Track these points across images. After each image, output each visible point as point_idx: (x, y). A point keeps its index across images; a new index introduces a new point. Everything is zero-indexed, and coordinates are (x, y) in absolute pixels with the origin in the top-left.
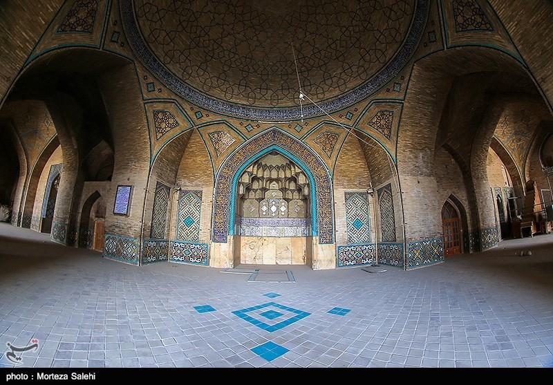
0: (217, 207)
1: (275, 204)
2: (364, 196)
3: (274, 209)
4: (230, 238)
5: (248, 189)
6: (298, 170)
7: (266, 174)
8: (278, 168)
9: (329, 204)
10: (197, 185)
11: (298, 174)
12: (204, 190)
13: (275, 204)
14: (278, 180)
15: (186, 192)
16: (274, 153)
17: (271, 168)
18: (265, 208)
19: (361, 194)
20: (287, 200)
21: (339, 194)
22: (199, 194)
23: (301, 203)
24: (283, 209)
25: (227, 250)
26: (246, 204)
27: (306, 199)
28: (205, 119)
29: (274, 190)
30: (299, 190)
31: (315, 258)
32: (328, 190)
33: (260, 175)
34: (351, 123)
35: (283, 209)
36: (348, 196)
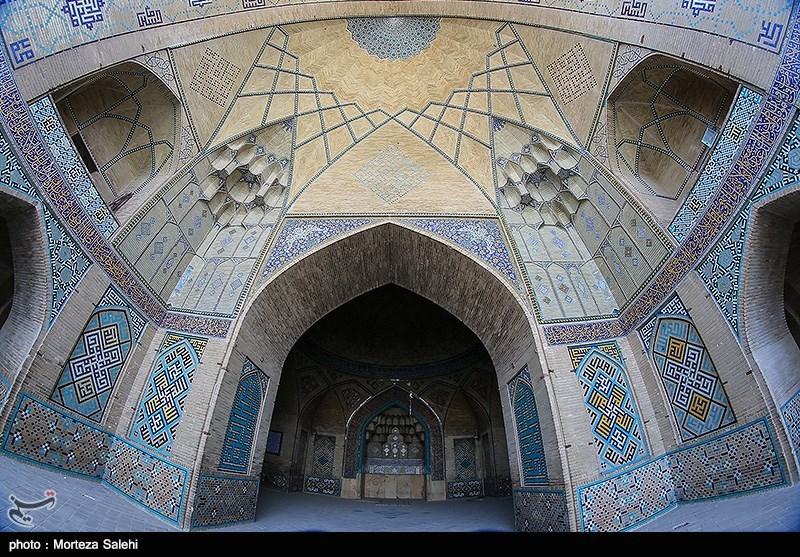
0: (348, 450)
1: (395, 446)
2: (472, 441)
3: (395, 451)
4: (359, 475)
5: (373, 434)
6: (415, 421)
7: (389, 422)
8: (399, 417)
9: (441, 450)
10: (332, 432)
11: (415, 424)
12: (337, 436)
13: (395, 446)
14: (399, 426)
15: (321, 436)
16: (396, 406)
17: (393, 417)
18: (387, 450)
19: (468, 439)
20: (407, 443)
21: (449, 441)
22: (332, 440)
23: (420, 446)
24: (404, 451)
25: (355, 484)
26: (370, 446)
27: (422, 443)
28: (339, 380)
29: (396, 437)
30: (418, 435)
31: (428, 491)
32: (439, 438)
33: (383, 423)
34: (457, 385)
35: (404, 451)
36: (457, 442)
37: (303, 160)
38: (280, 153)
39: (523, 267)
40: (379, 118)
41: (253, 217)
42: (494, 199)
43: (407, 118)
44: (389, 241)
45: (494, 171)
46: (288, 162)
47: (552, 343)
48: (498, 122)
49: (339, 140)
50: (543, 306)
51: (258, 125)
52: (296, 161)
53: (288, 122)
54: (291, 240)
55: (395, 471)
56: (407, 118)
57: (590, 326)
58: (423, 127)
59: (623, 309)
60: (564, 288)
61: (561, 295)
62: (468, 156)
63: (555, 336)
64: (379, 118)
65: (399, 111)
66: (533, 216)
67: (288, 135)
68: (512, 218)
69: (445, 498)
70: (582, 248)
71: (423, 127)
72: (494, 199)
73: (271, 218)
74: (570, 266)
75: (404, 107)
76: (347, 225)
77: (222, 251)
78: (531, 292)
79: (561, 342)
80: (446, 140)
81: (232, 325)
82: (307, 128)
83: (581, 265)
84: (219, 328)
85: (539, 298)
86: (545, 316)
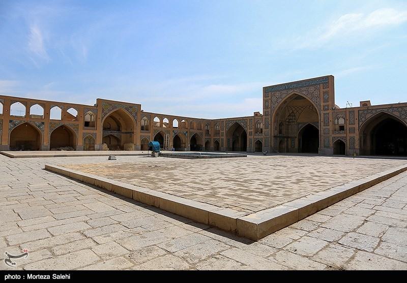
38: (294, 115)
41: (293, 123)
46: (295, 116)
49: (300, 111)
53: (293, 112)
84: (296, 137)
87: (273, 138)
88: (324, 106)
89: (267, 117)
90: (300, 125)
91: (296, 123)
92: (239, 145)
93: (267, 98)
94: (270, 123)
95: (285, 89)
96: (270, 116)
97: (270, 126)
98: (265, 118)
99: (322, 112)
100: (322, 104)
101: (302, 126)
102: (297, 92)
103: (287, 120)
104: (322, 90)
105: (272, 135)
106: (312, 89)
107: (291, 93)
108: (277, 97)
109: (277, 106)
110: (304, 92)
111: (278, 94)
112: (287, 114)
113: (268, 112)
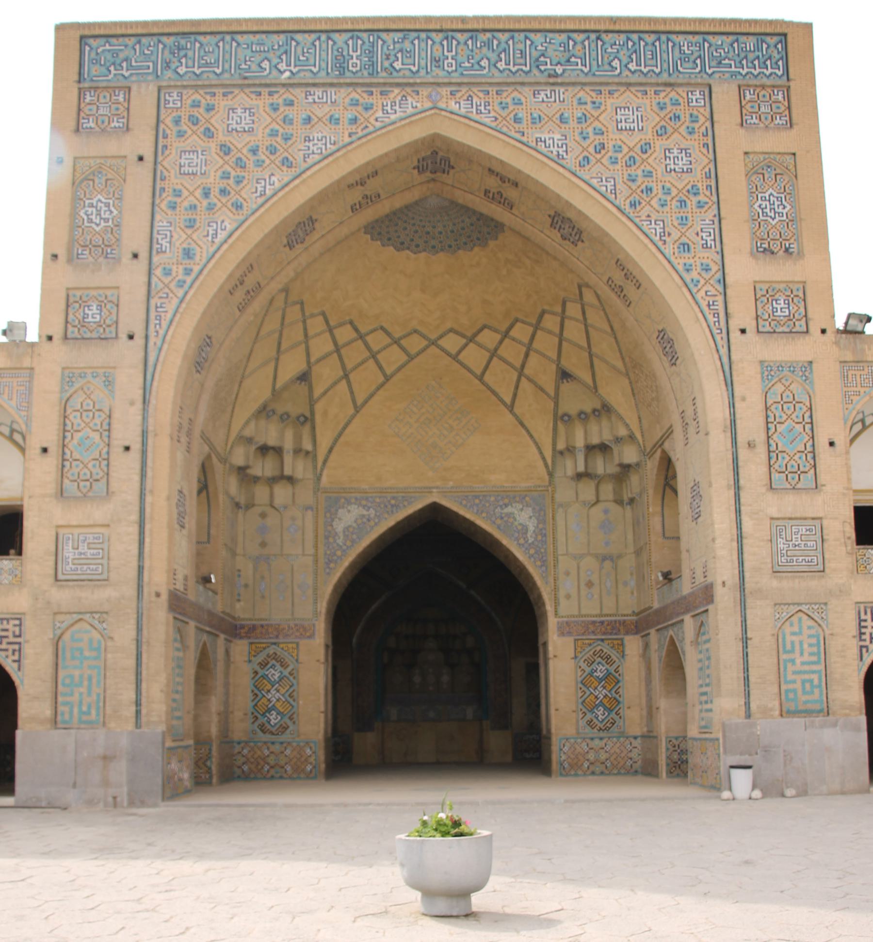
35: (445, 678)
37: (325, 413)
39: (556, 560)
40: (415, 344)
41: (282, 493)
42: (549, 462)
43: (452, 343)
44: (435, 509)
45: (555, 430)
46: (306, 420)
47: (562, 634)
48: (565, 375)
49: (366, 378)
50: (563, 602)
51: (267, 394)
52: (318, 418)
53: (304, 377)
54: (339, 527)
55: (432, 714)
56: (452, 343)
57: (602, 623)
58: (474, 357)
59: (638, 614)
60: (590, 584)
61: (584, 591)
62: (529, 404)
63: (565, 630)
64: (415, 344)
65: (440, 332)
66: (587, 490)
67: (303, 388)
68: (565, 492)
69: (509, 758)
70: (630, 537)
71: (474, 357)
72: (549, 462)
73: (305, 496)
74: (604, 558)
75: (448, 325)
76: (392, 506)
77: (263, 544)
78: (556, 589)
79: (570, 633)
80: (501, 378)
81: (317, 627)
82: (326, 374)
83: (620, 556)
84: (305, 632)
85: (562, 593)
86: (562, 610)
87: (160, 619)
88: (763, 294)
89: (93, 356)
90: (348, 517)
91: (305, 496)
92: (777, 568)
93: (111, 147)
94: (126, 429)
95: (340, 76)
96: (131, 353)
97: (126, 468)
98: (69, 377)
99: (750, 352)
100: (744, 270)
101: (358, 529)
102: (474, 124)
103: (239, 458)
104: (733, 141)
105: (158, 579)
106: (630, 115)
107: (399, 121)
108: (240, 143)
109: (223, 239)
110: (552, 136)
111: (243, 118)
112: (258, 390)
113: (111, 302)
